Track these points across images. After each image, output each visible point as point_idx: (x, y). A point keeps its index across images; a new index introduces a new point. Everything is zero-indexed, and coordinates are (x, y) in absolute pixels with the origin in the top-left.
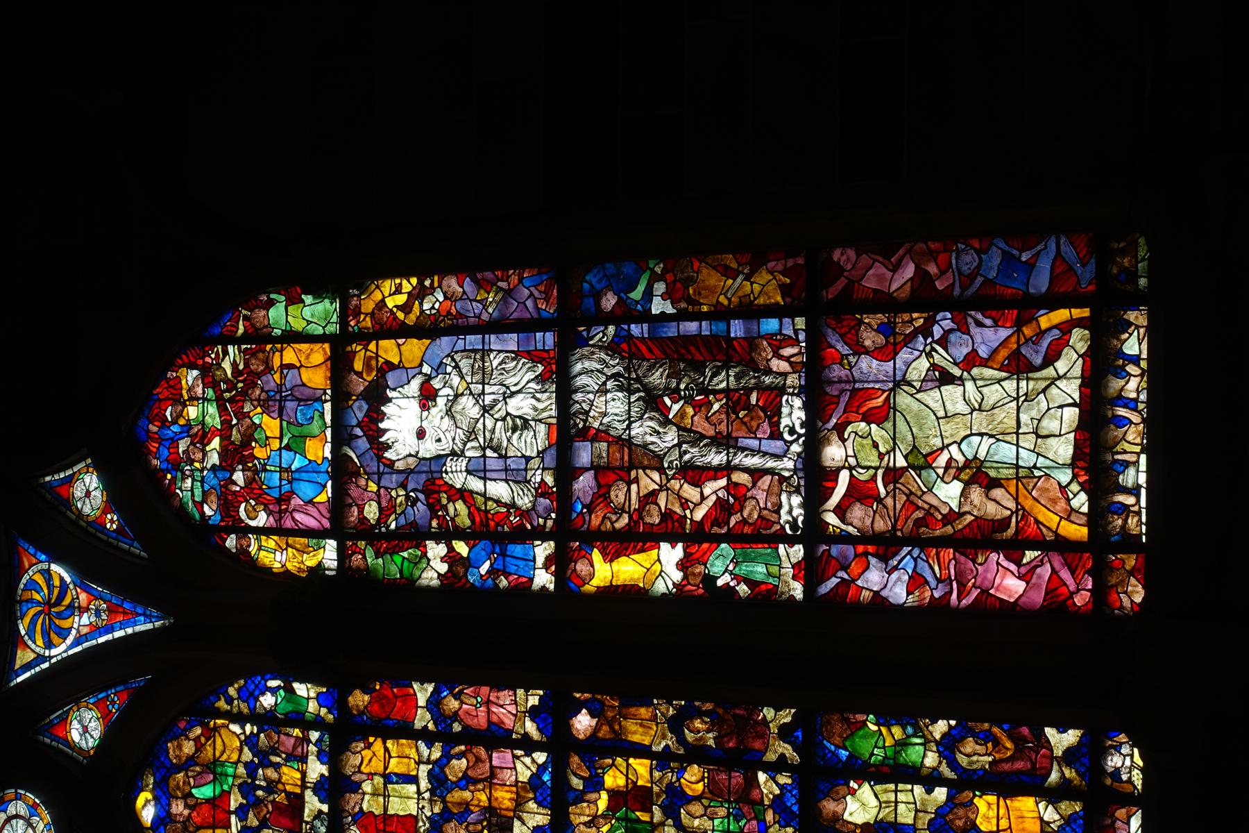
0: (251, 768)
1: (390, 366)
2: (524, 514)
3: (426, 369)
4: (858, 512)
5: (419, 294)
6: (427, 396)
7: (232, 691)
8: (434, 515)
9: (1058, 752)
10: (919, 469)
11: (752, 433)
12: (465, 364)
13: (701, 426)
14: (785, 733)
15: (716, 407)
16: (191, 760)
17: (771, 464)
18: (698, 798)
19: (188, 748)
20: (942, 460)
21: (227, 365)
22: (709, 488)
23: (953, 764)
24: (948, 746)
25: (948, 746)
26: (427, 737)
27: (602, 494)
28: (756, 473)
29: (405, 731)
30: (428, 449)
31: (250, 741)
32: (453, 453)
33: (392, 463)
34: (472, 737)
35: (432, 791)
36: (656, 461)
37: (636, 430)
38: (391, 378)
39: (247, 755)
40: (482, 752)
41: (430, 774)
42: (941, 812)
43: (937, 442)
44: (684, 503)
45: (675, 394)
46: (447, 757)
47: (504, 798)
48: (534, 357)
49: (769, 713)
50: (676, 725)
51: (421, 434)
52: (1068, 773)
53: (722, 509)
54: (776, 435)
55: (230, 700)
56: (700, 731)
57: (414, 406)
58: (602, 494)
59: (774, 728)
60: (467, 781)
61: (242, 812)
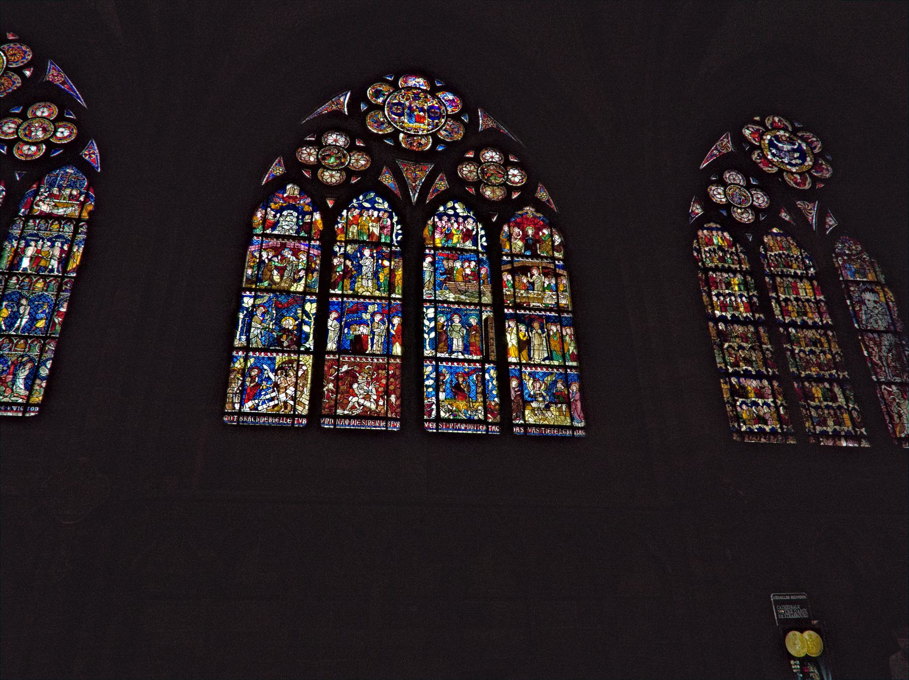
0: (793, 257)
1: (879, 294)
2: (862, 323)
3: (880, 302)
4: (886, 392)
5: (892, 301)
6: (875, 302)
7: (806, 253)
8: (856, 302)
9: (861, 430)
10: (897, 404)
11: (892, 371)
12: (883, 311)
13: (889, 361)
14: (844, 376)
15: (893, 364)
16: (789, 242)
17: (888, 375)
18: (826, 357)
19: (791, 242)
20: (900, 409)
21: (865, 256)
22: (879, 361)
23: (852, 410)
24: (854, 408)
25: (854, 408)
26: (815, 298)
27: (870, 339)
28: (885, 371)
29: (815, 295)
30: (867, 302)
31: (798, 257)
32: (867, 307)
33: (862, 293)
34: (818, 308)
35: (806, 299)
36: (880, 351)
37: (884, 347)
38: (877, 294)
39: (795, 256)
40: (817, 311)
41: (808, 299)
42: (843, 407)
43: (903, 408)
44: (875, 356)
45: (892, 355)
46: (813, 303)
47: (810, 315)
48: (889, 325)
49: (846, 373)
50: (837, 353)
51: (869, 300)
52: (859, 432)
53: (877, 365)
54: (893, 376)
55: (804, 252)
56: (838, 359)
57: (874, 299)
58: (870, 339)
59: (844, 374)
60: (811, 307)
61: (784, 254)
